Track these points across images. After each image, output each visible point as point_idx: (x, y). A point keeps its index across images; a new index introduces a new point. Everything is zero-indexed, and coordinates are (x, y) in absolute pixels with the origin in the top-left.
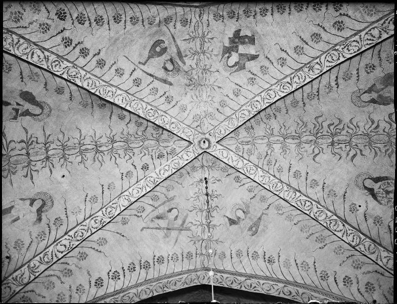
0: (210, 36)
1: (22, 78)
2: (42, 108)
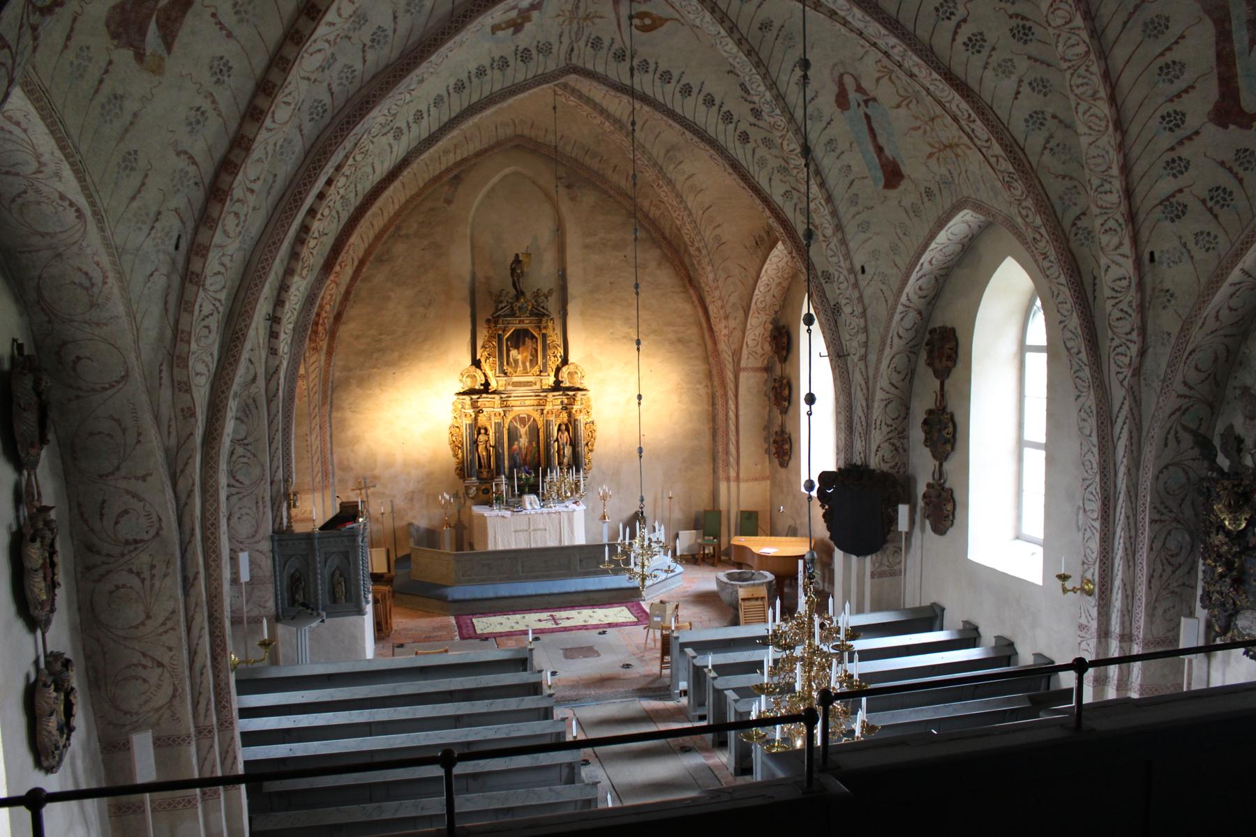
0: (562, 19)
1: (829, 123)
2: (842, 75)
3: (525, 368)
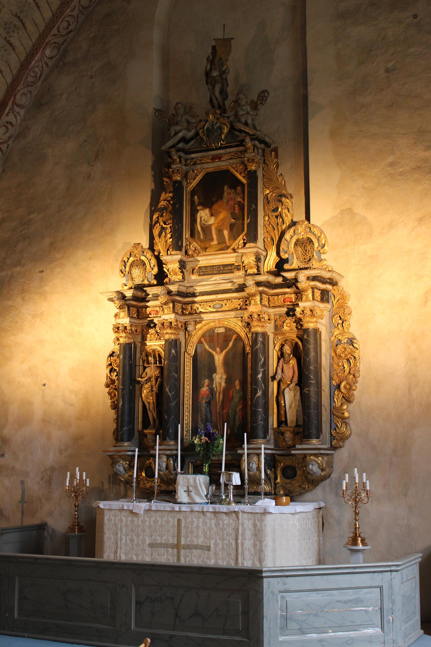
3: (221, 240)
